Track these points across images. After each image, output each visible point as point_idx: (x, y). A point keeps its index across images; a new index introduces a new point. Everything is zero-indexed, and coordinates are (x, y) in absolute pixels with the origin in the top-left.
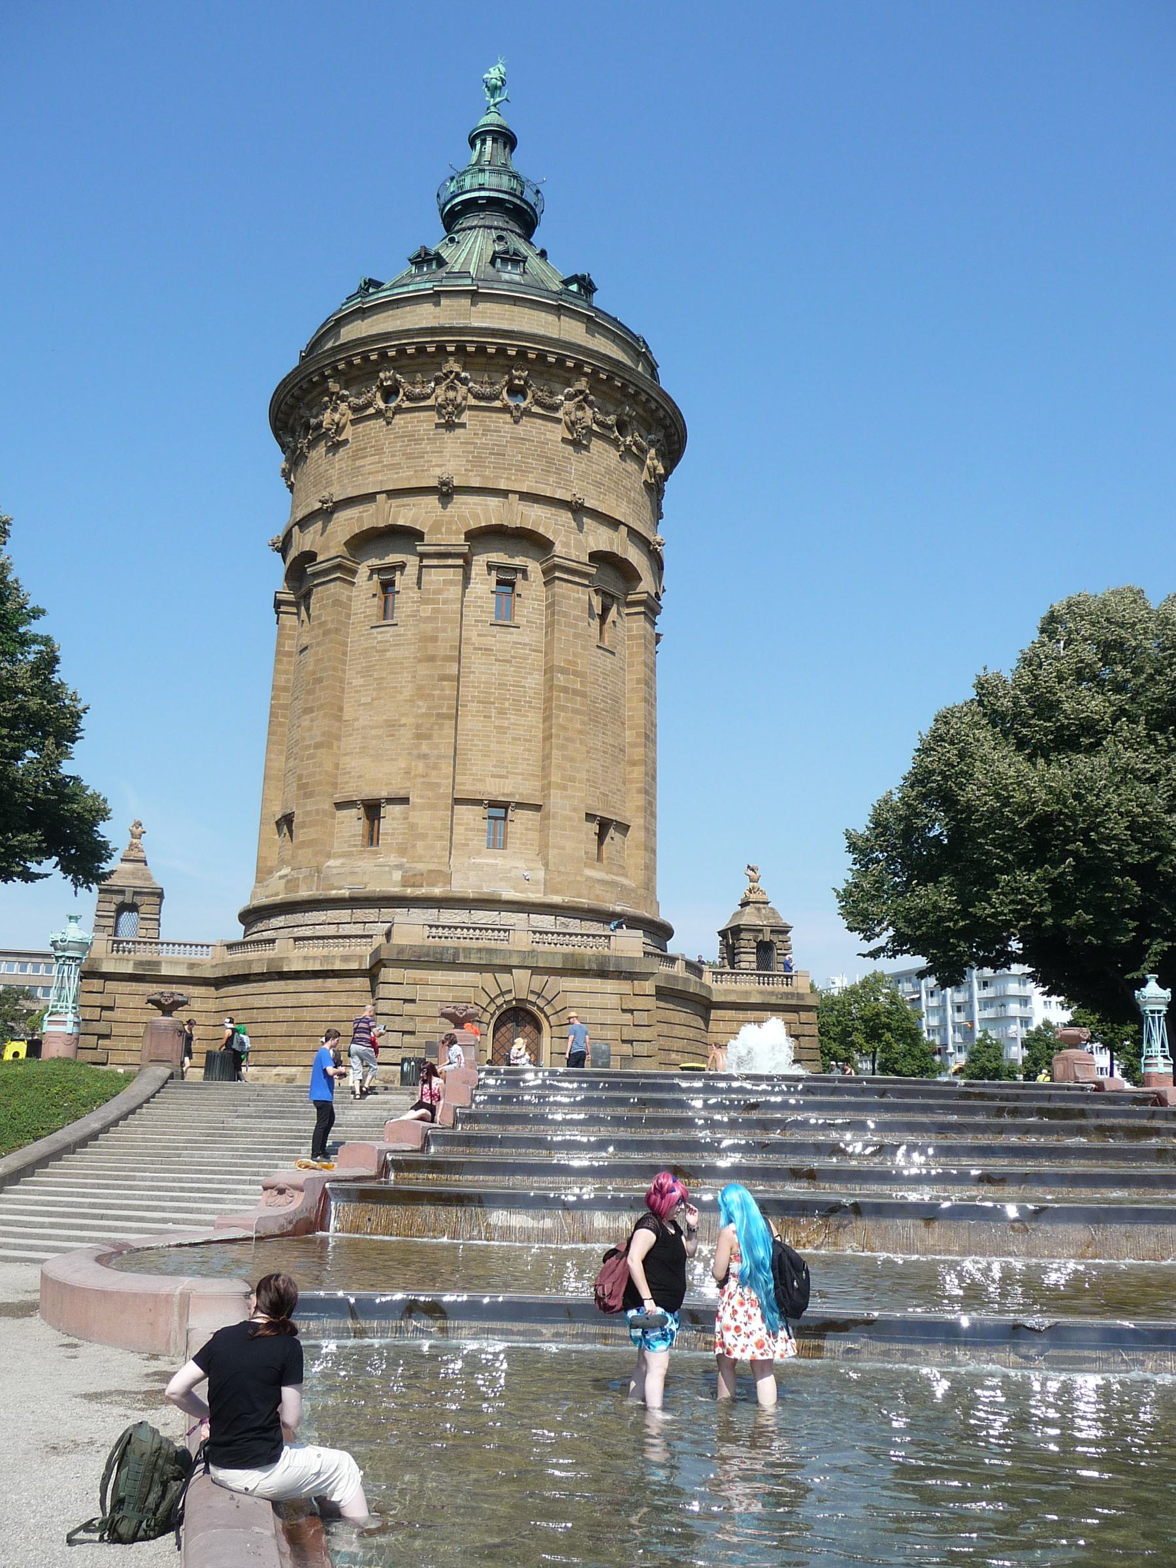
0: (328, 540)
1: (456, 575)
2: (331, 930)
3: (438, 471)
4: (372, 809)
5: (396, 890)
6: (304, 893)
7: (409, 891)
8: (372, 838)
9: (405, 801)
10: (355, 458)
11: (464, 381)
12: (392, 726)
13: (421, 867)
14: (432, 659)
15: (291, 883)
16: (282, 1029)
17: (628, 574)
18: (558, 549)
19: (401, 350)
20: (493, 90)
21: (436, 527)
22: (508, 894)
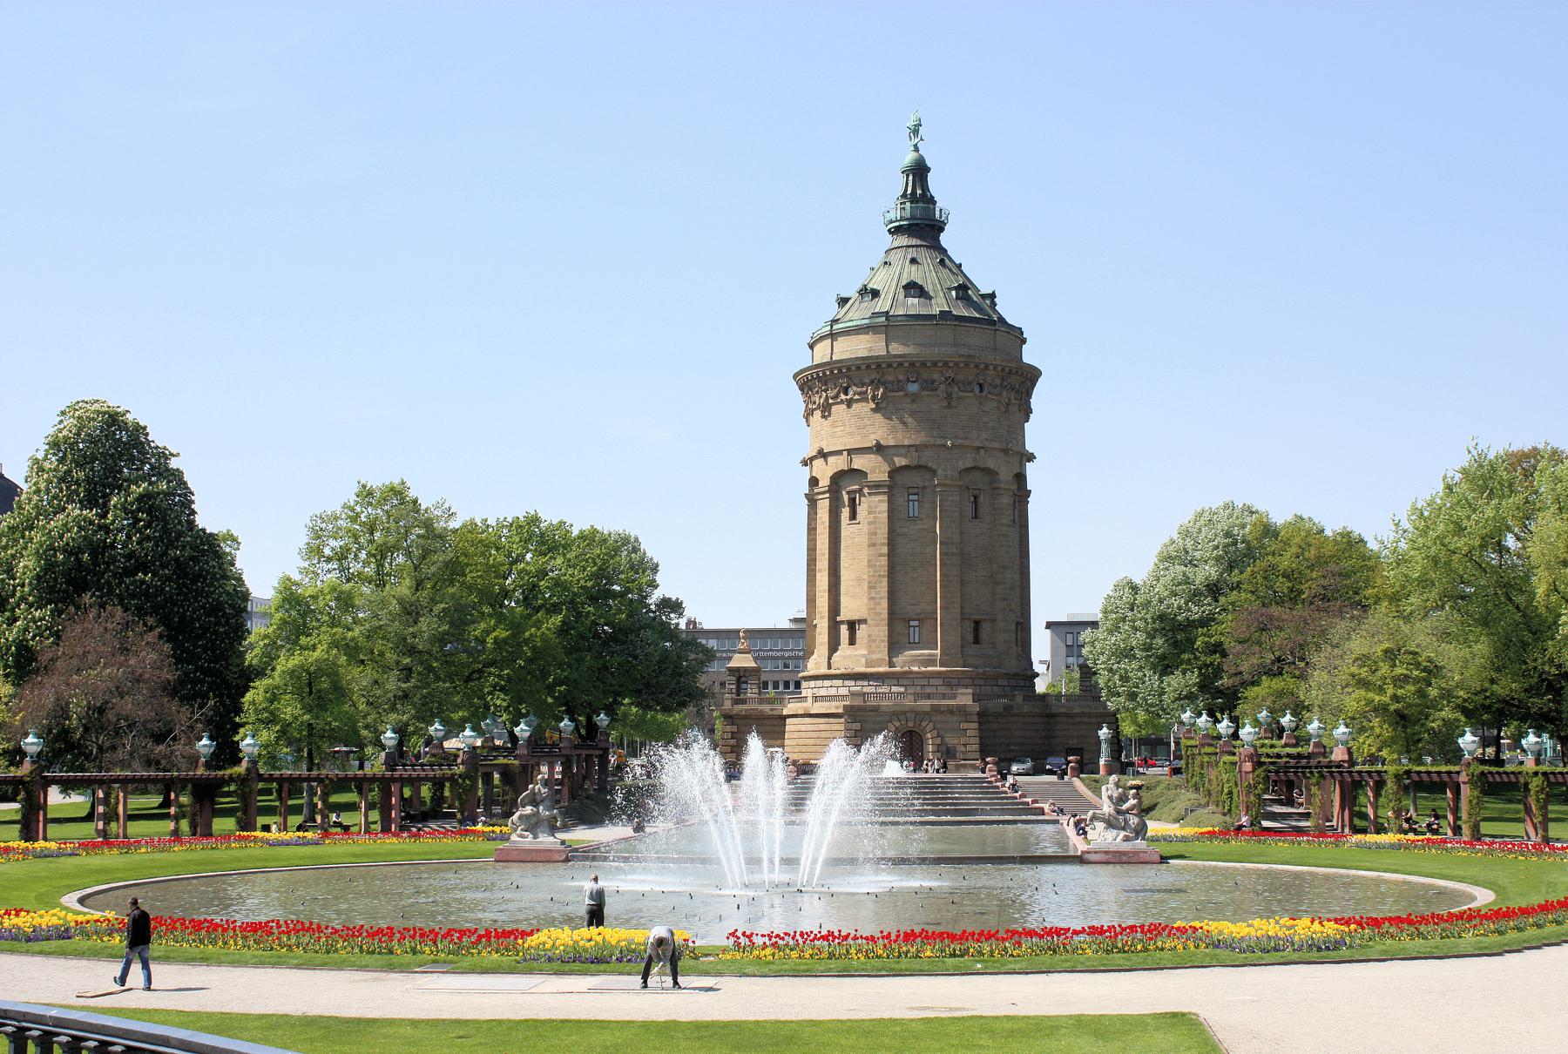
0: (824, 472)
1: (885, 498)
2: (833, 692)
3: (873, 437)
4: (852, 625)
5: (862, 669)
6: (824, 670)
7: (869, 670)
8: (852, 641)
9: (864, 621)
10: (833, 425)
11: (884, 384)
12: (859, 579)
13: (875, 657)
14: (874, 545)
15: (817, 665)
16: (812, 742)
17: (988, 471)
18: (940, 472)
19: (849, 369)
20: (915, 131)
21: (873, 471)
22: (915, 669)
